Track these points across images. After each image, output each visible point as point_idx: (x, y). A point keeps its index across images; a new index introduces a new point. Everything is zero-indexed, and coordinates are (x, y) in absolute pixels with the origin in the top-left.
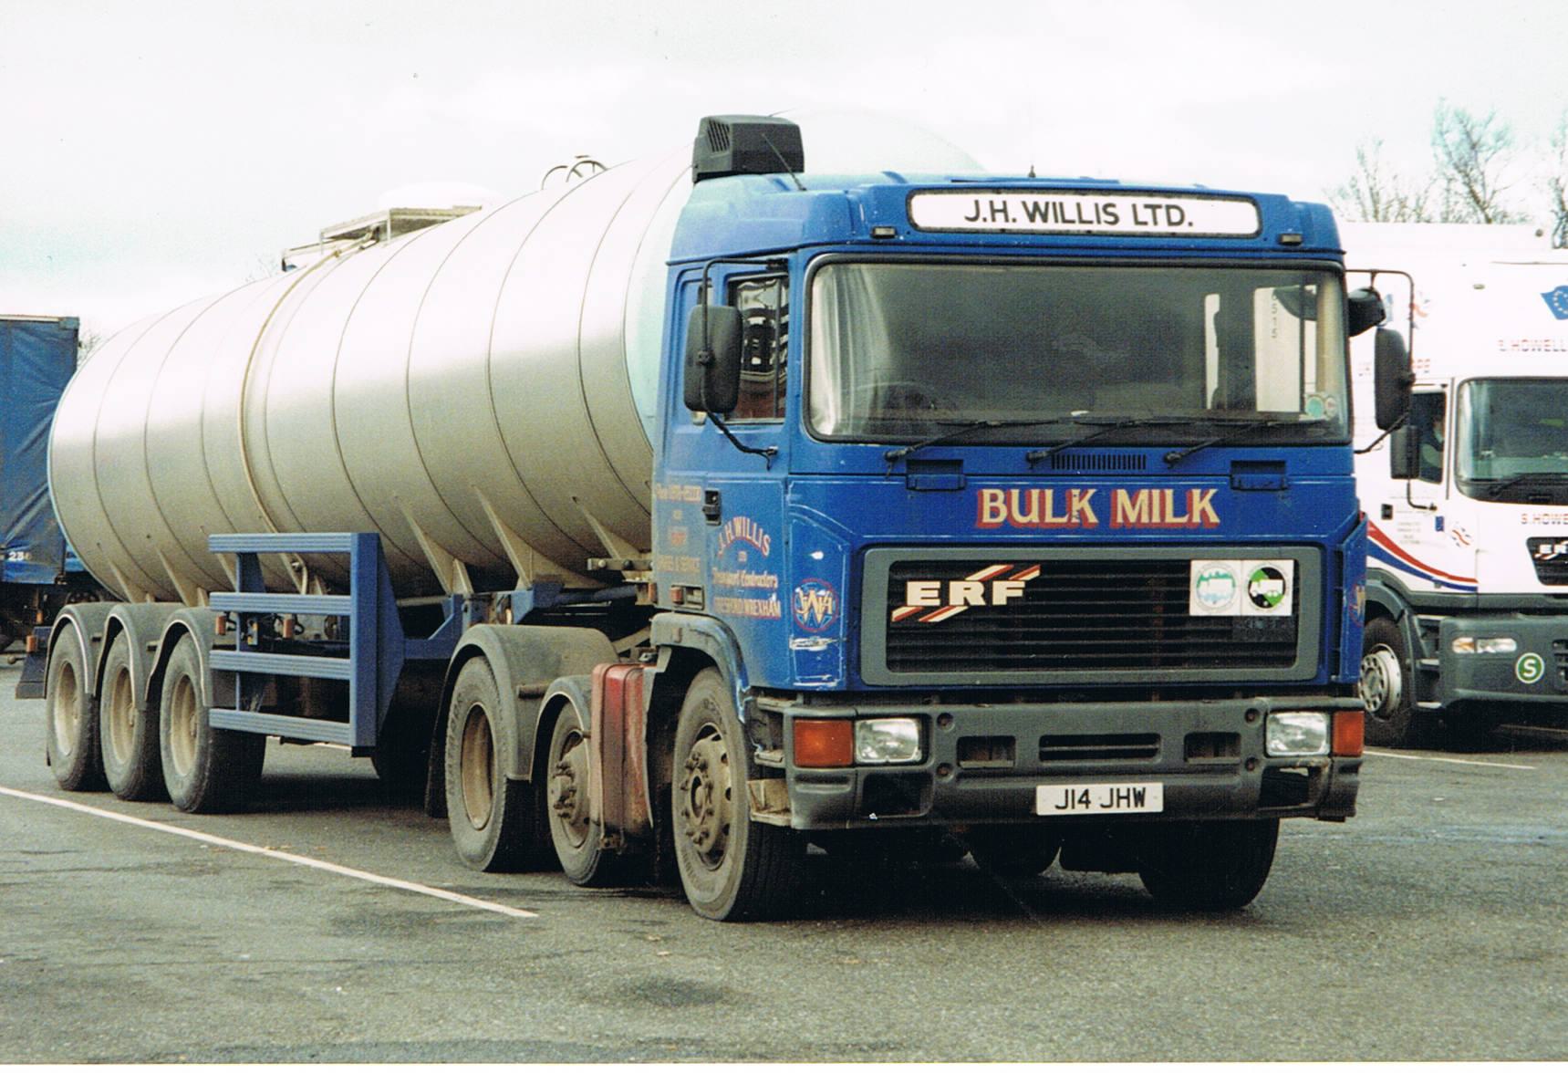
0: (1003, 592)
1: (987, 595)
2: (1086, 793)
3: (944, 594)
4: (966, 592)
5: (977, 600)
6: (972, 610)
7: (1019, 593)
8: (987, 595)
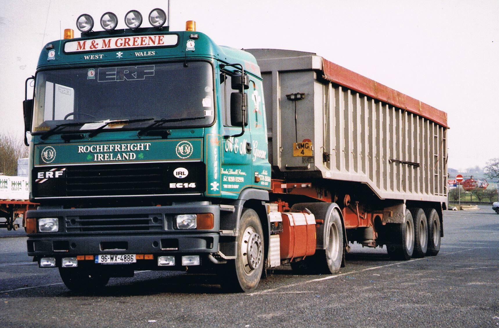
1: (54, 175)
4: (49, 174)
5: (51, 177)
8: (54, 175)
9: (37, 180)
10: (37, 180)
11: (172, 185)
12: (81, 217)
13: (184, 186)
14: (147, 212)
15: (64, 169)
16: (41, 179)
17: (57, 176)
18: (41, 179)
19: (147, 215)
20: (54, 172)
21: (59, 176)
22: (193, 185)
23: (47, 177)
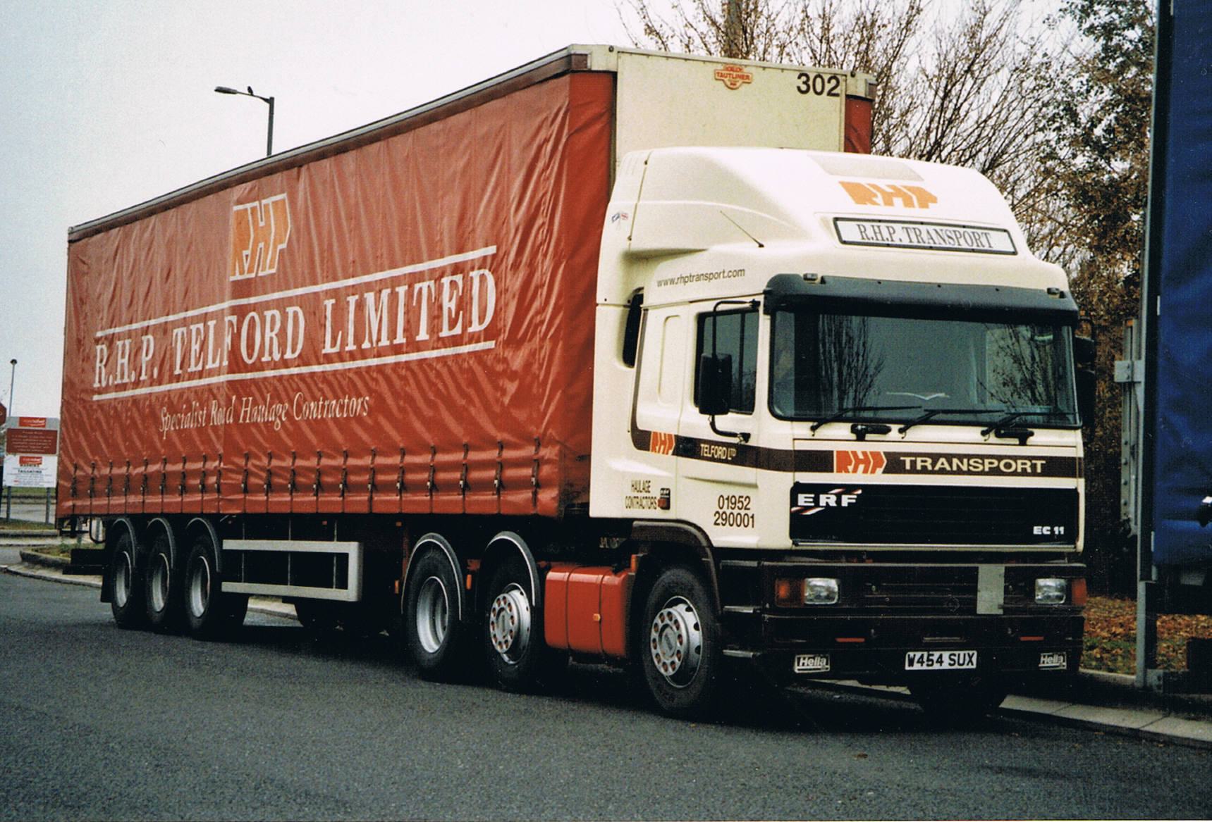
0: (845, 501)
1: (839, 501)
3: (816, 501)
4: (828, 500)
5: (832, 503)
8: (839, 501)
9: (794, 509)
10: (794, 509)
11: (1037, 530)
13: (1052, 531)
17: (845, 503)
22: (1059, 530)
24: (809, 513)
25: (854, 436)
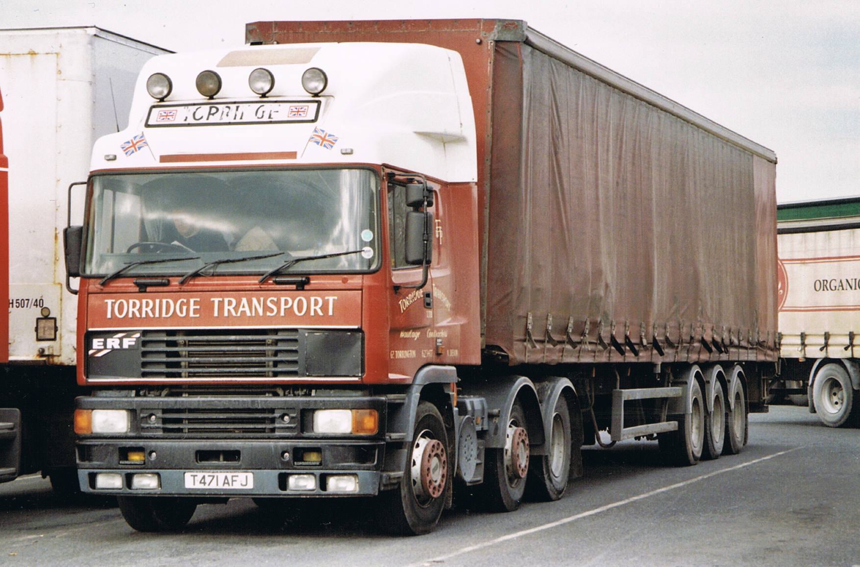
0: (127, 343)
1: (121, 344)
2: (204, 477)
4: (113, 343)
5: (117, 346)
6: (113, 349)
7: (133, 343)
8: (121, 344)
9: (91, 352)
12: (165, 411)
14: (270, 406)
15: (138, 335)
16: (99, 351)
18: (99, 351)
19: (272, 411)
20: (121, 339)
21: (129, 346)
23: (109, 346)
24: (100, 355)
25: (137, 289)
